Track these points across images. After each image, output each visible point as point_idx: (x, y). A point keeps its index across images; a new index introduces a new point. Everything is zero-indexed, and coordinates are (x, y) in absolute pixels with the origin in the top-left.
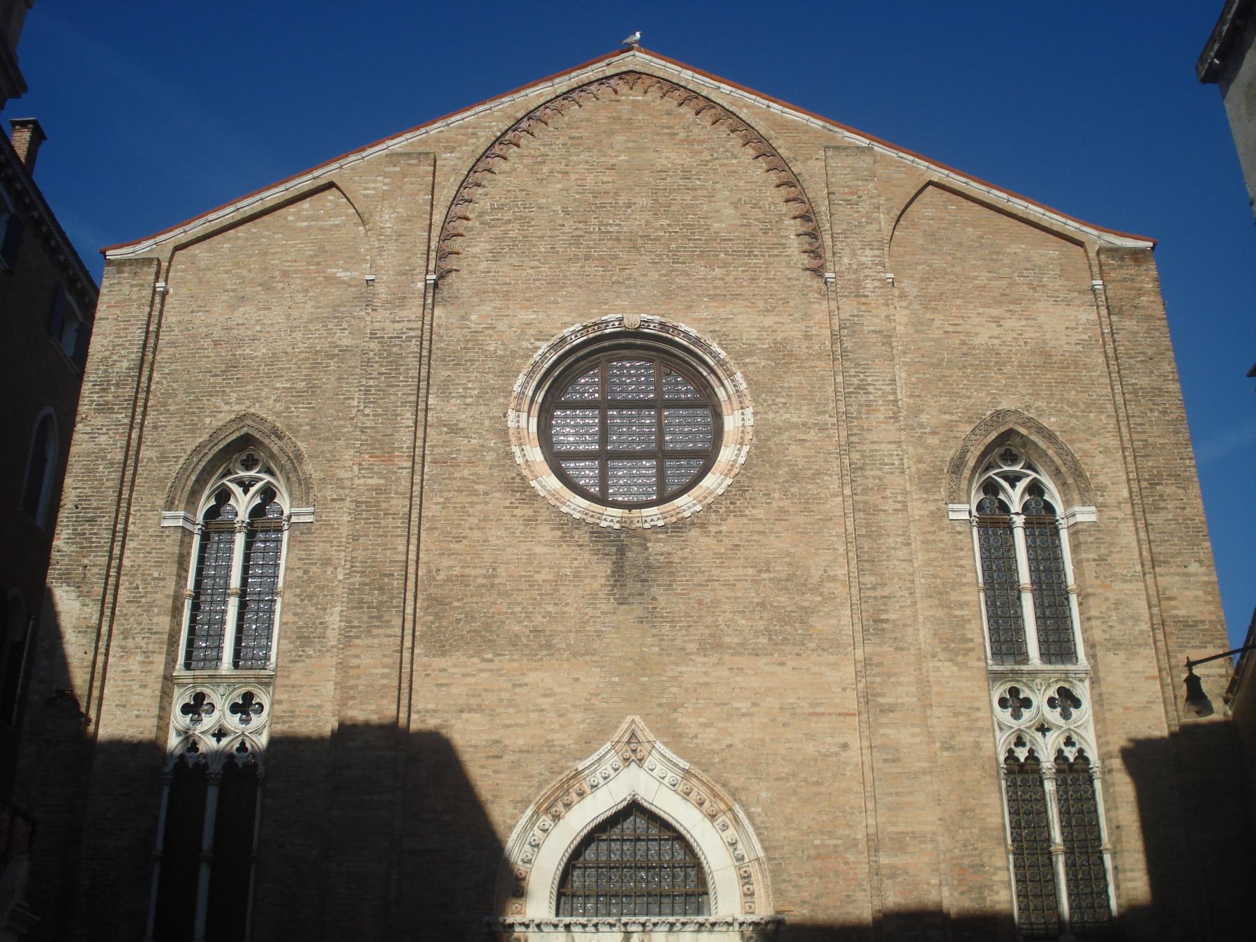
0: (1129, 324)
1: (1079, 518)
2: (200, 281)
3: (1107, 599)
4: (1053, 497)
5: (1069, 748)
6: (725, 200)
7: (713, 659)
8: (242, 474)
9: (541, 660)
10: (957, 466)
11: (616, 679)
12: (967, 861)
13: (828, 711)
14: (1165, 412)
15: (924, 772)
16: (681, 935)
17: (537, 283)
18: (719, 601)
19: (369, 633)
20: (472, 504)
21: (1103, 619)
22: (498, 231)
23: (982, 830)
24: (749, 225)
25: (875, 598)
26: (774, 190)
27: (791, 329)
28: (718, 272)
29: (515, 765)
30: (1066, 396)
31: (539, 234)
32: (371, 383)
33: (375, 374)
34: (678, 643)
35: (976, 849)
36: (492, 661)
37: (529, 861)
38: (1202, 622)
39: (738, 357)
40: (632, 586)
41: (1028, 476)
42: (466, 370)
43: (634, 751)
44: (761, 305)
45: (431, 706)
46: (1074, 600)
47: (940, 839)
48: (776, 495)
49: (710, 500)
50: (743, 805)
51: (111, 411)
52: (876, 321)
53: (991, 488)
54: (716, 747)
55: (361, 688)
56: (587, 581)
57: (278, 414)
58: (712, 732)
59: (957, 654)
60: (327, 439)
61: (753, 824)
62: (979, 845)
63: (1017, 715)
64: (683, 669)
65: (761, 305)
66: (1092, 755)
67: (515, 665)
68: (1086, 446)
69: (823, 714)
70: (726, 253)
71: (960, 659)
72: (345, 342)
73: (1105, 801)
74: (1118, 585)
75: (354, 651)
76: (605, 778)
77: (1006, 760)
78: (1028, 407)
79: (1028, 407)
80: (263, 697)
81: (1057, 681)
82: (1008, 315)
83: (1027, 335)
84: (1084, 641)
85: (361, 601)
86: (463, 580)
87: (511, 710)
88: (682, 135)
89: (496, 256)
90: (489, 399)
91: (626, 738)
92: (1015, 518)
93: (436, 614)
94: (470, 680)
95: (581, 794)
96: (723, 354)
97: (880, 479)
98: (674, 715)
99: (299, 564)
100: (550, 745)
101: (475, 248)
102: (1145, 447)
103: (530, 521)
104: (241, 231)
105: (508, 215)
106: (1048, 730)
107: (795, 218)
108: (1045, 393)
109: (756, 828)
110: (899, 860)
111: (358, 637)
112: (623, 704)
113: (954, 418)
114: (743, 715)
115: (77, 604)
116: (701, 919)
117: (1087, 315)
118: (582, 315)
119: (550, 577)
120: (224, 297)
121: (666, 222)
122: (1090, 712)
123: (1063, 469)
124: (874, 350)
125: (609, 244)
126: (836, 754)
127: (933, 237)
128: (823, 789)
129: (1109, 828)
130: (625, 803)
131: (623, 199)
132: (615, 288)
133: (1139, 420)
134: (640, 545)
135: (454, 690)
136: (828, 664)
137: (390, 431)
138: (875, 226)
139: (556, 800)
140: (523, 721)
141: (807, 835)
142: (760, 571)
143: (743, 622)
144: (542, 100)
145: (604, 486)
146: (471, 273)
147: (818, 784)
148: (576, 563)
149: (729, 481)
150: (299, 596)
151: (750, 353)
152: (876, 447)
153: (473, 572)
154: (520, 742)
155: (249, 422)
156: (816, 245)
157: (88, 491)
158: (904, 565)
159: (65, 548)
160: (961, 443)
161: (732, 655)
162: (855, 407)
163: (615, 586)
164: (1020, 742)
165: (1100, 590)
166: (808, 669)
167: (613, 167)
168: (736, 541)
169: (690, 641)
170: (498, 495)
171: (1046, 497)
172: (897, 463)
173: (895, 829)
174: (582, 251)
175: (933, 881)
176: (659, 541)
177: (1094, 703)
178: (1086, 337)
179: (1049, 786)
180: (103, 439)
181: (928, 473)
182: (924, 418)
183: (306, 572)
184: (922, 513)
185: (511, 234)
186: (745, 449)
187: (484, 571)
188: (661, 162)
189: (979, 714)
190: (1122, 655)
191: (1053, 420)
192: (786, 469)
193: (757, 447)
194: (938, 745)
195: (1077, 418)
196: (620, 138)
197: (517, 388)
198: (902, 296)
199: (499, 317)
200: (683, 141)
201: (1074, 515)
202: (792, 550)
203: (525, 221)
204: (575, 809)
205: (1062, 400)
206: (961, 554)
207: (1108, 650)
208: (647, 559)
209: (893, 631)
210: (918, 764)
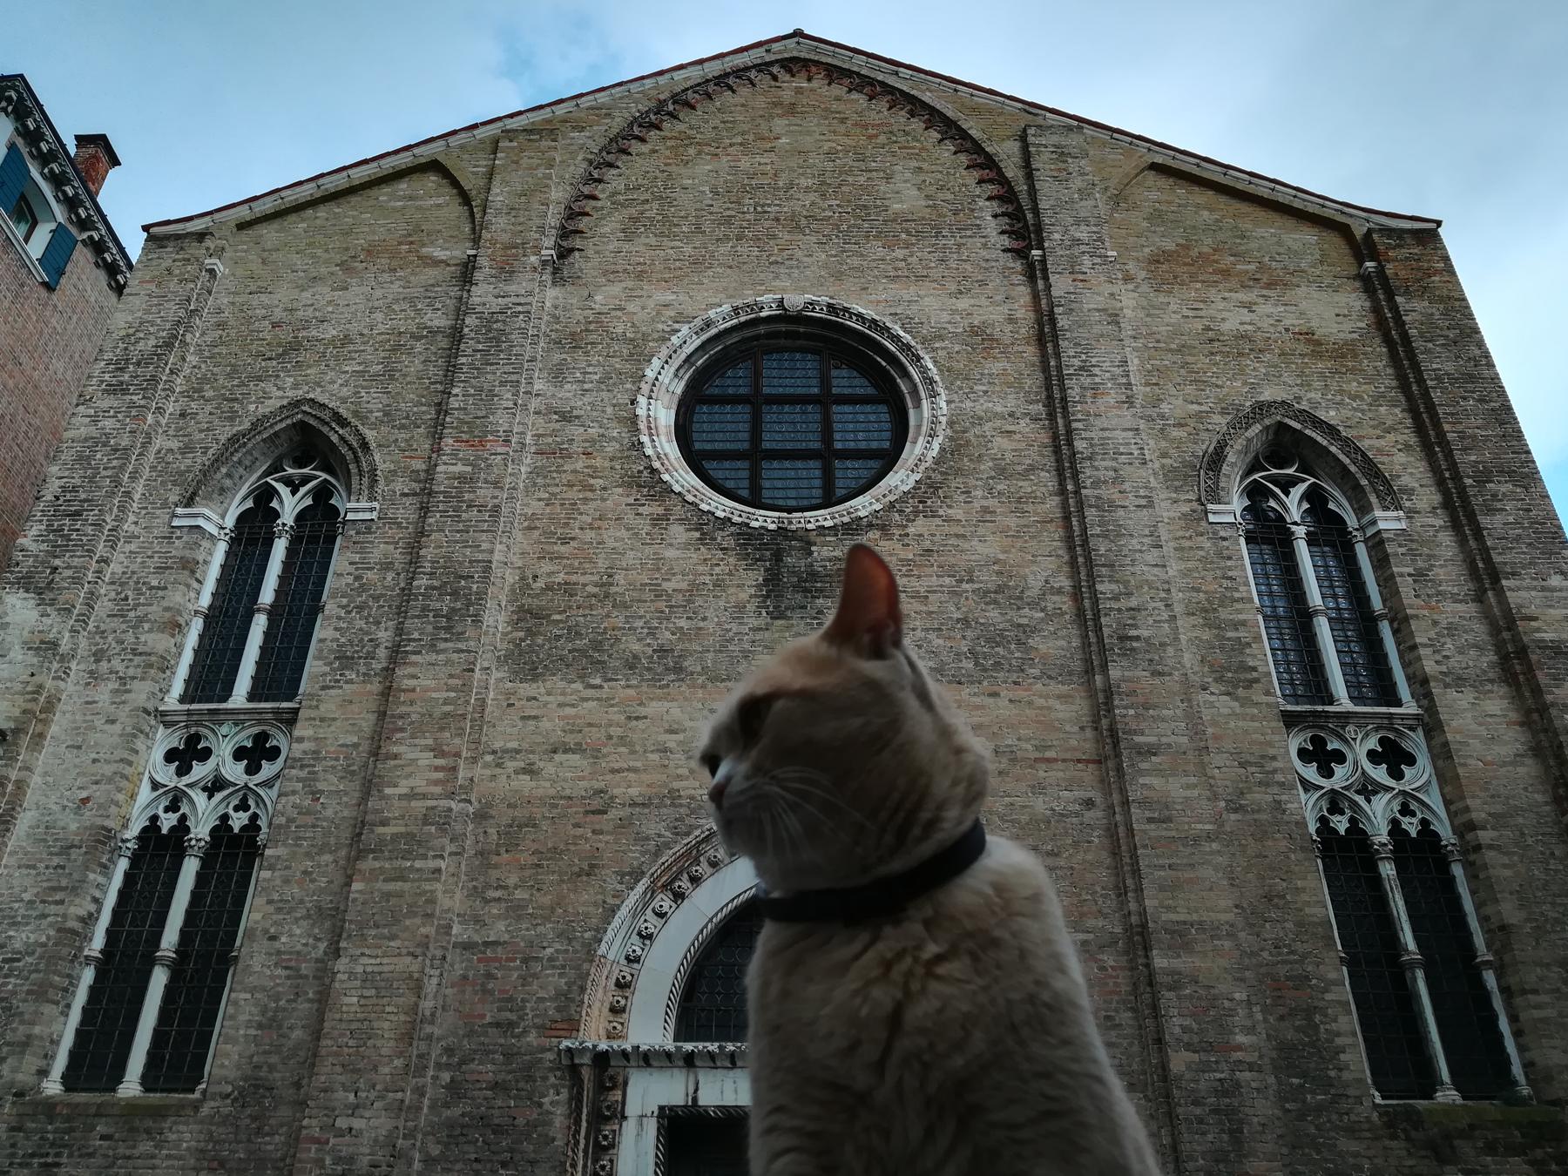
2: (264, 262)
3: (1435, 623)
4: (1340, 505)
8: (290, 471)
10: (1216, 460)
12: (1282, 971)
15: (1209, 837)
19: (432, 647)
23: (1299, 924)
24: (934, 207)
25: (1119, 610)
26: (964, 173)
28: (900, 253)
29: (623, 824)
32: (463, 360)
33: (469, 351)
35: (1292, 952)
36: (601, 687)
37: (637, 960)
41: (1304, 480)
42: (586, 353)
45: (513, 745)
47: (1242, 935)
49: (892, 498)
51: (125, 392)
53: (1256, 493)
55: (414, 717)
56: (731, 590)
57: (344, 401)
59: (1236, 687)
60: (403, 427)
62: (1298, 946)
67: (631, 692)
68: (1382, 442)
69: (1056, 760)
70: (909, 234)
72: (436, 323)
73: (1473, 893)
74: (1449, 607)
75: (410, 670)
78: (1298, 399)
79: (1298, 399)
80: (279, 740)
81: (1377, 729)
82: (1261, 300)
83: (1287, 322)
84: (1408, 678)
85: (425, 609)
86: (568, 589)
89: (628, 234)
92: (1294, 528)
93: (529, 630)
94: (569, 711)
96: (907, 338)
99: (351, 569)
100: (674, 795)
101: (605, 231)
103: (657, 520)
104: (322, 212)
105: (647, 196)
106: (1375, 793)
107: (989, 199)
110: (1183, 963)
111: (419, 653)
113: (1204, 408)
115: (35, 614)
118: (731, 297)
119: (684, 585)
120: (291, 276)
122: (1429, 769)
123: (1353, 469)
124: (1097, 329)
125: (767, 224)
126: (1077, 814)
129: (1488, 932)
134: (802, 548)
135: (545, 724)
136: (1059, 697)
137: (480, 414)
139: (681, 873)
140: (639, 764)
142: (961, 581)
143: (941, 641)
144: (689, 83)
146: (597, 252)
150: (343, 607)
151: (941, 338)
152: (1107, 434)
153: (582, 579)
154: (634, 791)
155: (306, 408)
157: (77, 481)
159: (33, 547)
163: (768, 596)
164: (1335, 808)
165: (1426, 612)
166: (1030, 703)
168: (927, 544)
171: (1331, 506)
173: (1174, 917)
175: (1237, 996)
177: (1434, 758)
179: (1388, 870)
180: (108, 424)
183: (357, 578)
184: (1172, 514)
187: (596, 578)
189: (1276, 764)
191: (1332, 413)
193: (951, 439)
194: (1223, 804)
195: (1363, 411)
197: (650, 374)
198: (1128, 279)
199: (630, 298)
202: (1001, 556)
204: (706, 886)
205: (1341, 392)
206: (1229, 563)
207: (1447, 686)
210: (1199, 826)
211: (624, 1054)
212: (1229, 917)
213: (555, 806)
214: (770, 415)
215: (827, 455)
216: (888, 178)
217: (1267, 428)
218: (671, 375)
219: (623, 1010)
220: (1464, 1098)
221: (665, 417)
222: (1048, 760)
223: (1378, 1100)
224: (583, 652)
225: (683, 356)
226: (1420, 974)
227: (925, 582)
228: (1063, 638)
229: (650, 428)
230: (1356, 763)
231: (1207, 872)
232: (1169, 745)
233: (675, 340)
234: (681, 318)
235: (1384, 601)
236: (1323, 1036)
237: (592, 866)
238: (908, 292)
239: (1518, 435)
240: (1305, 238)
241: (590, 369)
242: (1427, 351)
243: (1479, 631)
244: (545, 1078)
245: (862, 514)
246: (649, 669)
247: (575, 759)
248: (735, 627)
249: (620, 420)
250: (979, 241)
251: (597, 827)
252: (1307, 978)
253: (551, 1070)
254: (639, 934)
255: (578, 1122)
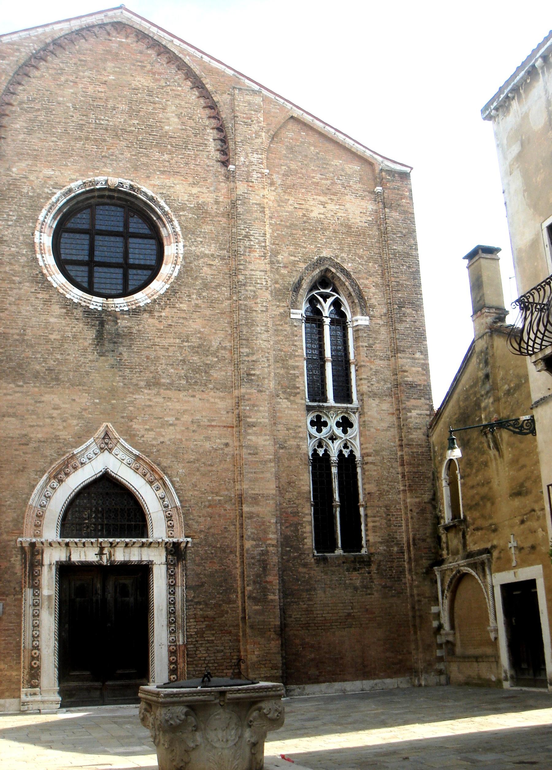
0: (395, 215)
1: (360, 323)
3: (371, 369)
5: (346, 450)
6: (173, 112)
7: (155, 391)
9: (52, 387)
10: (297, 287)
11: (97, 401)
12: (290, 510)
13: (218, 424)
14: (409, 267)
16: (132, 549)
17: (55, 152)
18: (159, 358)
20: (11, 289)
21: (368, 379)
22: (31, 115)
23: (299, 493)
24: (186, 130)
25: (248, 361)
27: (208, 198)
28: (166, 157)
29: (37, 449)
30: (357, 251)
31: (58, 120)
34: (134, 381)
35: (295, 503)
36: (22, 386)
37: (45, 506)
38: (420, 385)
39: (176, 210)
40: (108, 346)
41: (333, 296)
42: (9, 203)
43: (107, 444)
44: (191, 180)
46: (353, 369)
48: (194, 296)
49: (155, 297)
50: (169, 477)
52: (258, 197)
53: (312, 301)
54: (154, 442)
56: (81, 341)
58: (152, 434)
59: (290, 395)
61: (174, 487)
62: (297, 501)
63: (319, 431)
64: (137, 396)
65: (191, 180)
66: (358, 454)
67: (37, 389)
68: (366, 282)
69: (216, 426)
71: (292, 398)
73: (363, 479)
74: (378, 362)
76: (89, 459)
77: (312, 455)
78: (337, 257)
79: (337, 257)
82: (329, 201)
83: (339, 214)
87: (34, 417)
88: (149, 67)
90: (23, 223)
91: (102, 436)
94: (9, 397)
95: (75, 468)
96: (167, 208)
97: (254, 292)
98: (131, 424)
100: (57, 438)
102: (398, 285)
103: (47, 302)
106: (335, 439)
107: (213, 129)
108: (346, 249)
109: (176, 490)
110: (255, 509)
112: (101, 416)
113: (297, 259)
114: (171, 425)
116: (144, 540)
117: (371, 206)
118: (82, 175)
119: (58, 337)
121: (136, 122)
122: (357, 430)
123: (353, 294)
124: (255, 215)
125: (102, 132)
126: (222, 449)
127: (291, 149)
128: (214, 469)
130: (101, 473)
131: (110, 104)
132: (104, 160)
133: (395, 270)
134: (113, 321)
136: (220, 398)
138: (259, 141)
139: (60, 471)
140: (41, 424)
141: (204, 494)
142: (183, 341)
144: (62, 33)
145: (91, 282)
146: (13, 140)
147: (211, 465)
148: (74, 330)
149: (167, 286)
152: (253, 273)
153: (11, 331)
154: (39, 436)
156: (225, 147)
158: (265, 343)
160: (299, 275)
161: (165, 389)
162: (242, 248)
163: (98, 345)
164: (320, 445)
165: (368, 364)
166: (208, 400)
167: (105, 83)
168: (170, 322)
169: (141, 380)
170: (27, 284)
171: (342, 309)
172: (264, 283)
173: (253, 492)
174: (83, 134)
175: (272, 521)
176: (124, 319)
177: (360, 426)
178: (370, 219)
179: (334, 470)
181: (280, 290)
182: (280, 257)
185: (40, 118)
186: (178, 267)
187: (18, 331)
188: (135, 84)
189: (300, 430)
190: (377, 401)
191: (350, 265)
192: (200, 281)
193: (184, 267)
195: (362, 265)
196: (110, 65)
197: (41, 218)
198: (272, 184)
200: (149, 71)
201: (357, 321)
202: (202, 330)
203: (48, 111)
205: (355, 254)
207: (370, 397)
208: (117, 329)
209: (257, 381)
211: (42, 543)
212: (274, 492)
213: (6, 441)
214: (99, 240)
215: (126, 266)
216: (164, 109)
217: (321, 271)
218: (51, 218)
219: (40, 525)
220: (344, 552)
221: (47, 240)
222: (213, 426)
223: (316, 554)
224: (13, 368)
225: (57, 208)
226: (338, 509)
227: (168, 341)
228: (224, 371)
229: (41, 250)
230: (331, 428)
231: (268, 475)
232: (260, 423)
233: (54, 199)
234: (57, 186)
235: (355, 356)
236: (300, 533)
237: (24, 468)
238: (168, 182)
239: (418, 286)
240: (355, 167)
241: (11, 213)
242: (393, 240)
243: (388, 374)
244: (11, 551)
245: (142, 304)
246: (44, 378)
247: (13, 419)
248: (82, 359)
249: (27, 244)
250: (205, 154)
251: (25, 451)
252: (298, 513)
253: (13, 548)
254: (45, 496)
255: (25, 567)
